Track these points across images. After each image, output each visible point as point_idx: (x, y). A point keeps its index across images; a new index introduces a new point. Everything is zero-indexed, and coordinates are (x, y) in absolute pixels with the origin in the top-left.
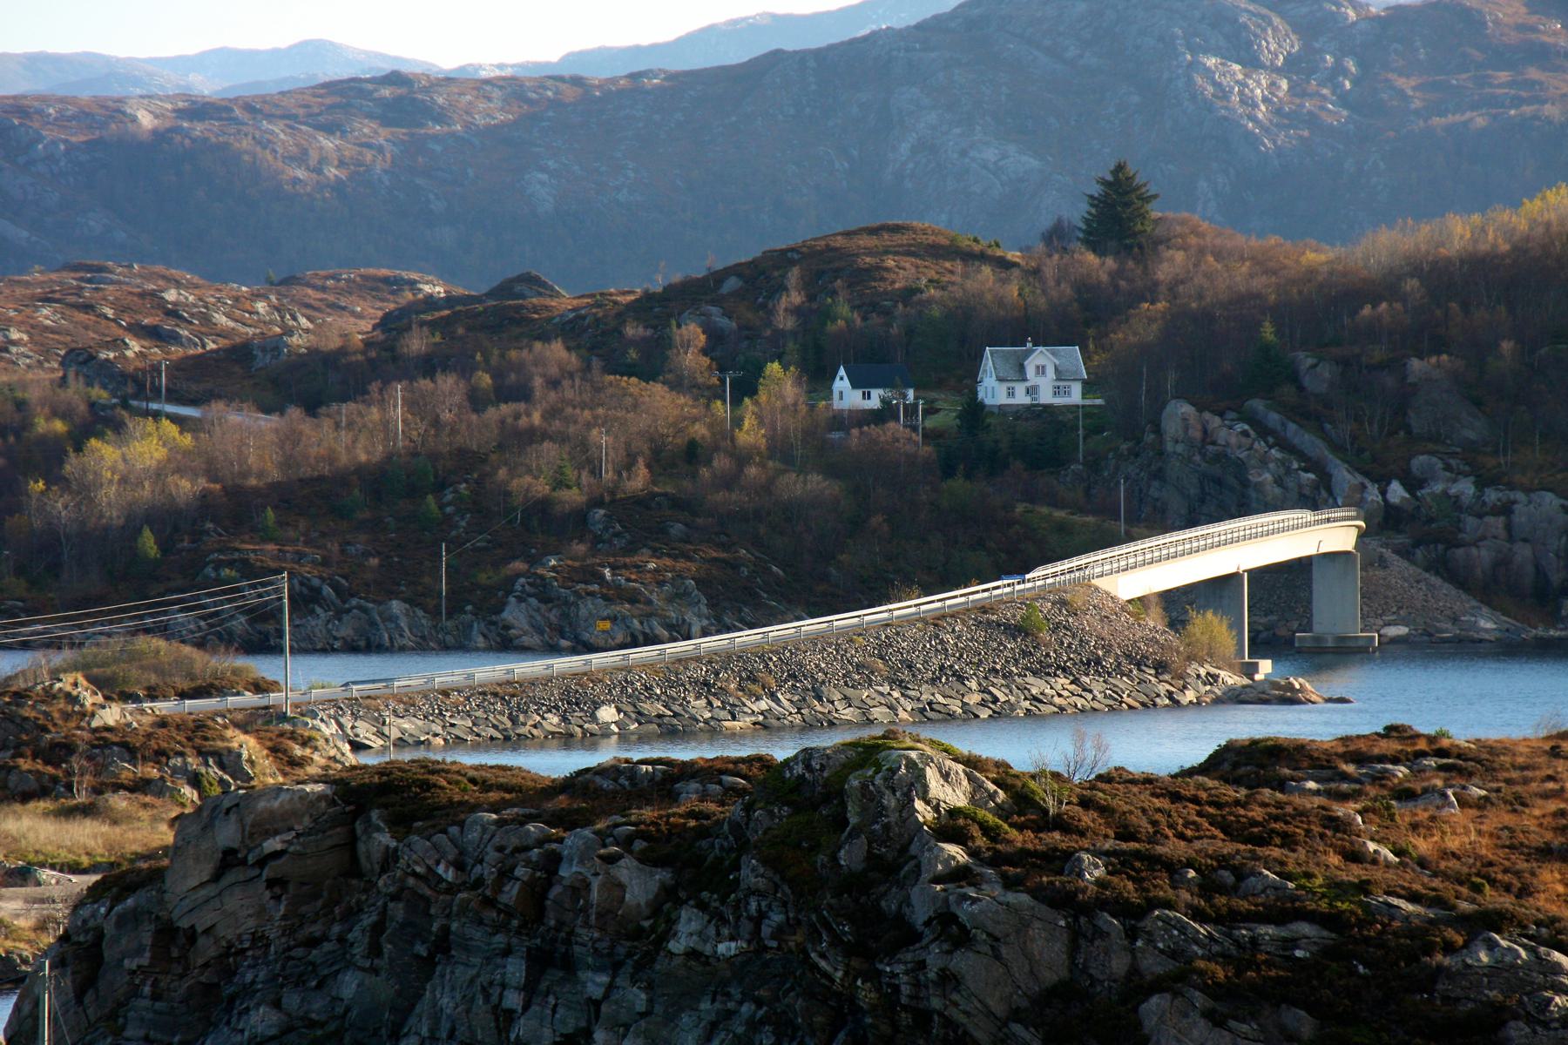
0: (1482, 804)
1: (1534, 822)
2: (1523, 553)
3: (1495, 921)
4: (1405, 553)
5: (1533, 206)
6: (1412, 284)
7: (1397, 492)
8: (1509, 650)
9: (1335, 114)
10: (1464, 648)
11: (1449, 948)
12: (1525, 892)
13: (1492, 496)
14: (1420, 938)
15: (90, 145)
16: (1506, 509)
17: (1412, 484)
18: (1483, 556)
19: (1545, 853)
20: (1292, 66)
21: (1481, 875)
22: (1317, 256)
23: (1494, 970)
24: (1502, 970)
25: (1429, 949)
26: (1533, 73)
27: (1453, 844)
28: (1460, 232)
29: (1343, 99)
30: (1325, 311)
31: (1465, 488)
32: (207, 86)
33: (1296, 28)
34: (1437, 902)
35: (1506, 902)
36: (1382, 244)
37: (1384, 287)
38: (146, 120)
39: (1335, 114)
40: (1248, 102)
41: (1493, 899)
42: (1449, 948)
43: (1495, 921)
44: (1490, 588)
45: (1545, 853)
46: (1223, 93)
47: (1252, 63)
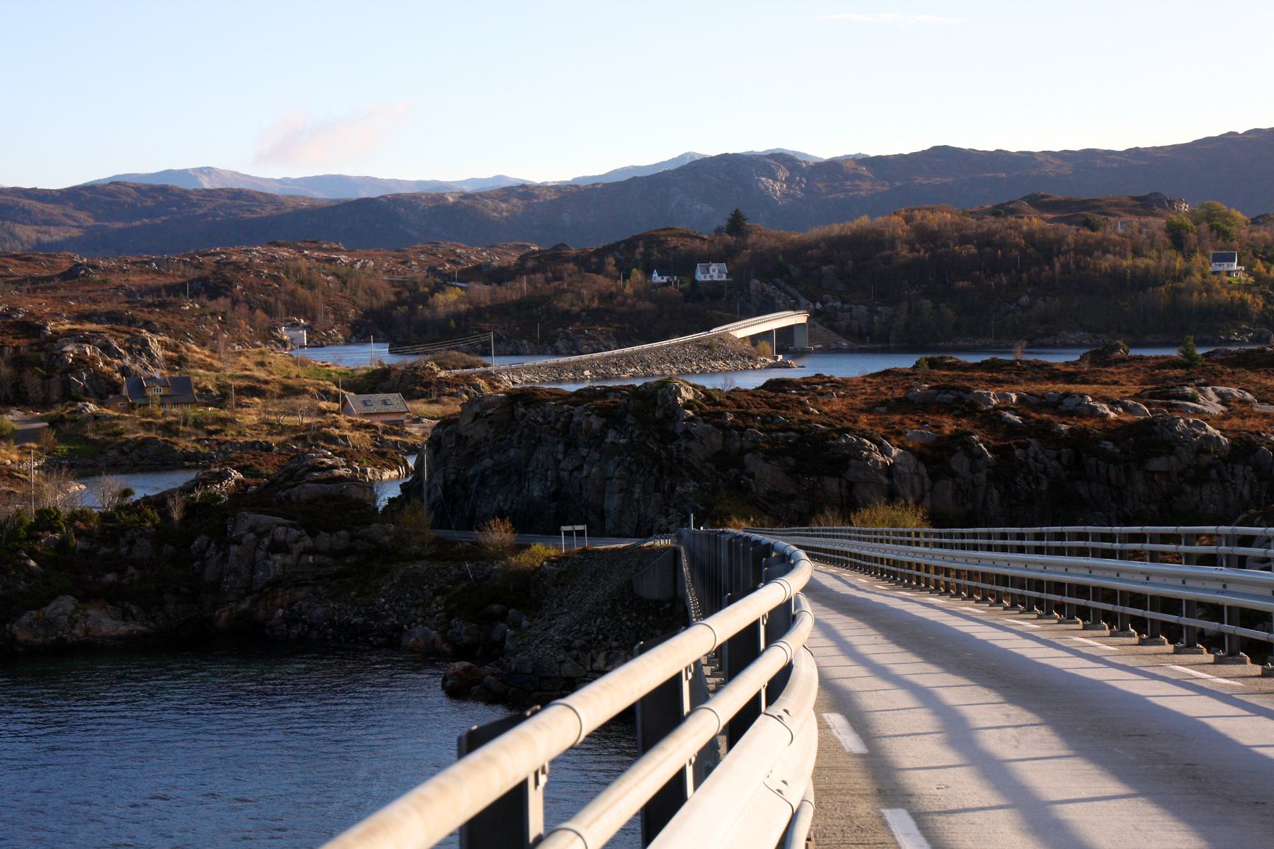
0: (843, 396)
1: (858, 402)
2: (855, 323)
3: (847, 430)
4: (821, 323)
5: (857, 221)
6: (823, 244)
7: (819, 306)
8: (851, 351)
9: (800, 194)
10: (838, 351)
11: (834, 439)
12: (856, 422)
13: (846, 306)
14: (825, 435)
15: (435, 207)
16: (850, 310)
17: (823, 303)
18: (843, 324)
19: (861, 411)
20: (787, 180)
21: (842, 417)
22: (795, 236)
23: (846, 445)
24: (849, 445)
25: (828, 439)
26: (857, 182)
27: (835, 408)
28: (836, 229)
29: (802, 190)
30: (798, 252)
31: (838, 304)
32: (468, 189)
33: (788, 169)
34: (830, 425)
35: (850, 425)
36: (814, 232)
37: (815, 245)
38: (451, 199)
39: (800, 194)
40: (774, 191)
41: (846, 424)
42: (834, 439)
43: (847, 430)
44: (846, 334)
45: (861, 411)
46: (767, 188)
47: (775, 179)
